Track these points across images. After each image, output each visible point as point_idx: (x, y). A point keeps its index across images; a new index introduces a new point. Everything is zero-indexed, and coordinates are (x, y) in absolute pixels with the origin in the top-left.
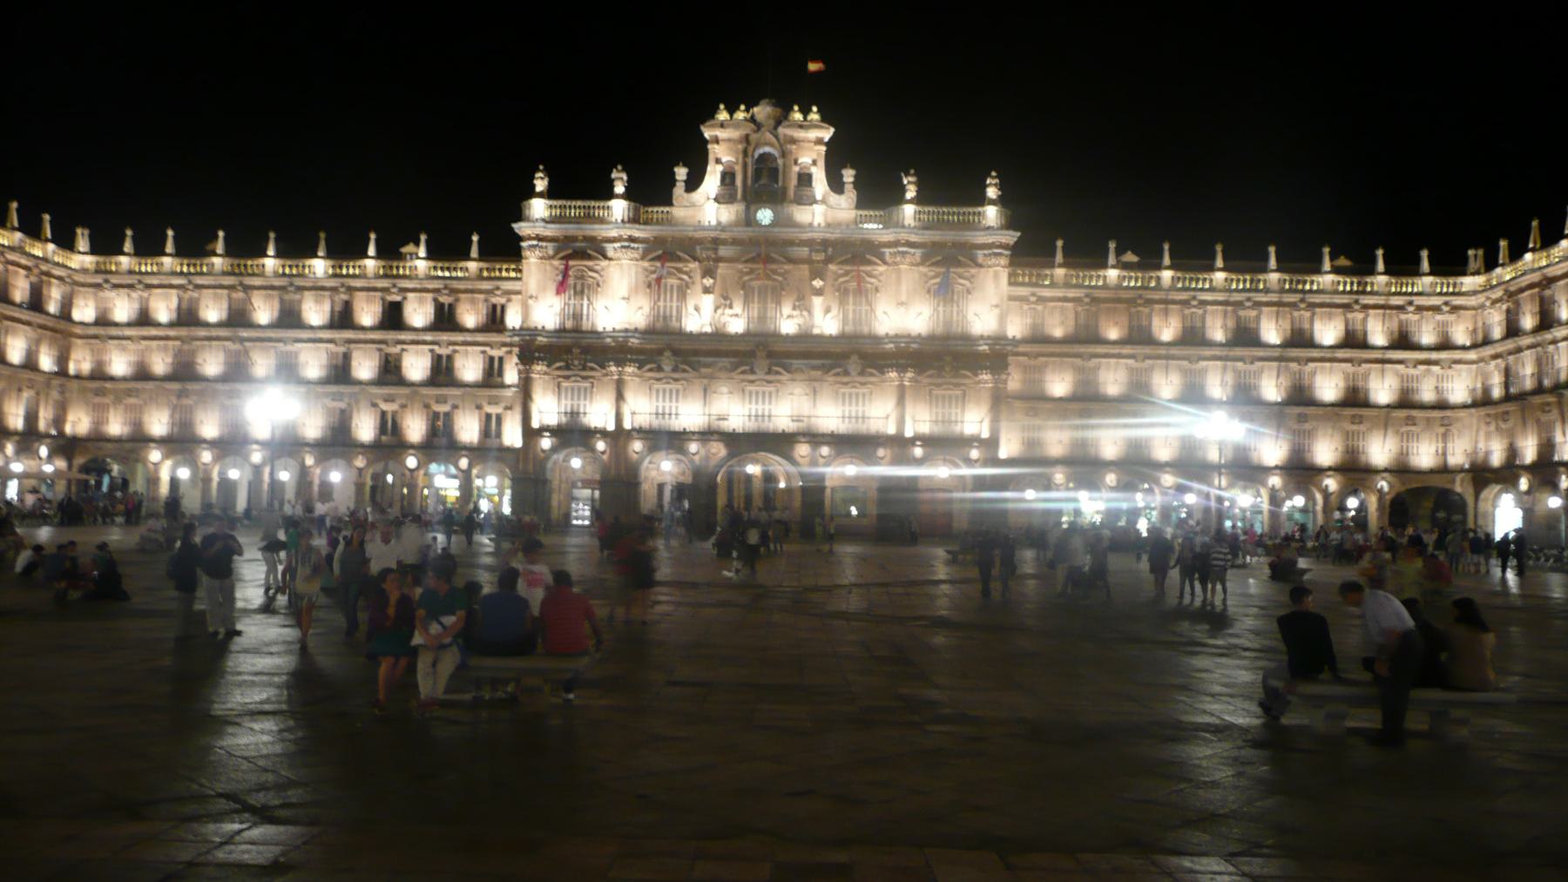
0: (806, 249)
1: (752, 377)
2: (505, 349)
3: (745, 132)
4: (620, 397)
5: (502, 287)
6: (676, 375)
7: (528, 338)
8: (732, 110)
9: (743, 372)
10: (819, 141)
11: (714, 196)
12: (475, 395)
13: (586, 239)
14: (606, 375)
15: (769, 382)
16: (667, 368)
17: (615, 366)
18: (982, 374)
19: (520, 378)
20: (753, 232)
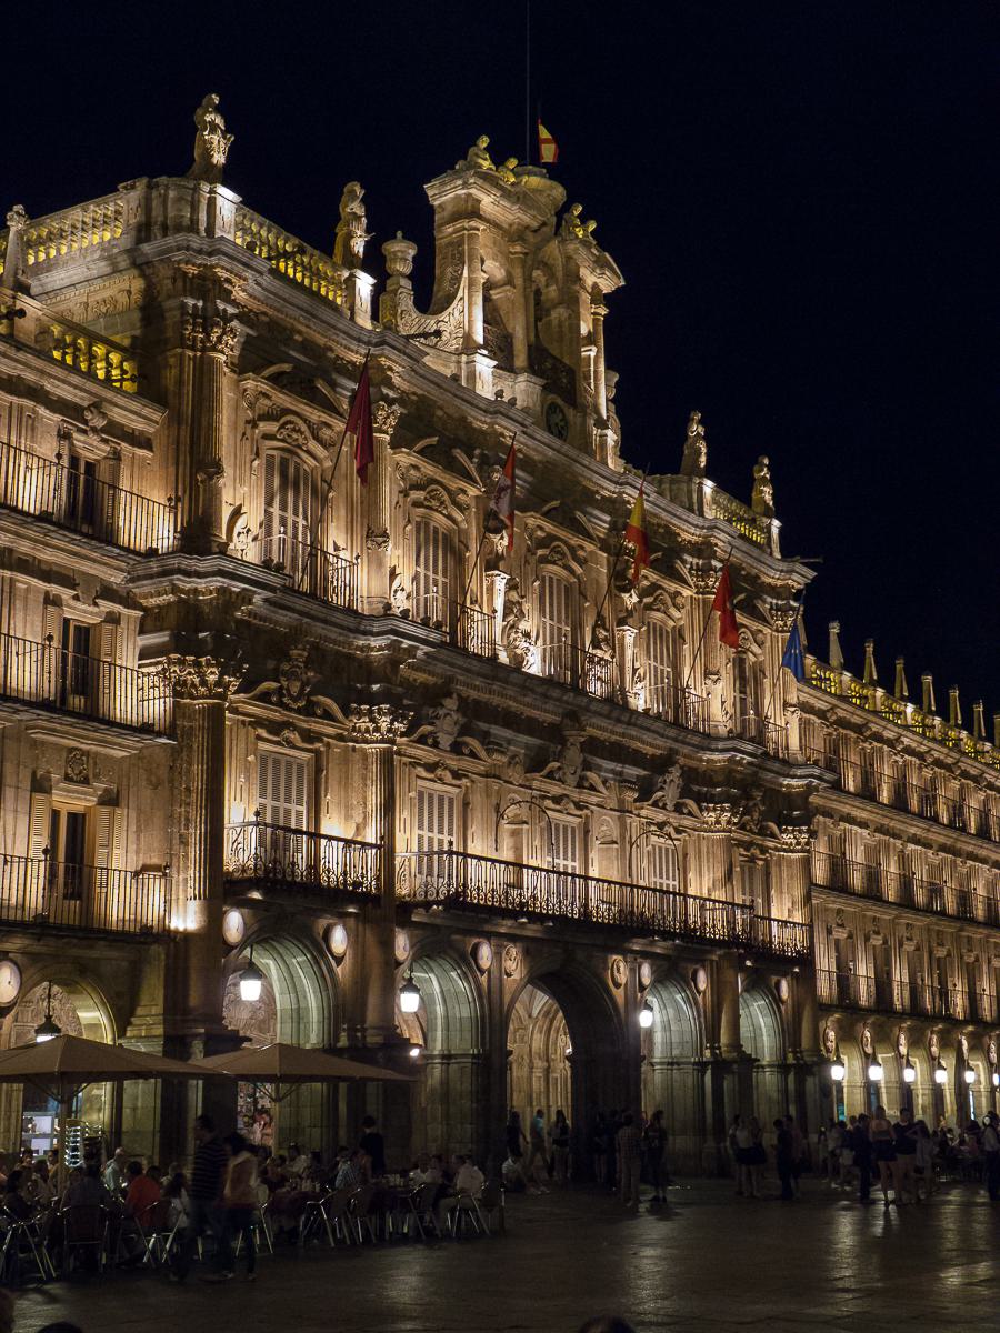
0: (608, 518)
1: (556, 790)
2: (106, 606)
3: (527, 219)
4: (388, 808)
5: (107, 408)
6: (453, 762)
7: (237, 587)
8: (499, 161)
9: (550, 775)
10: (597, 296)
11: (479, 338)
12: (34, 744)
13: (308, 347)
14: (340, 738)
15: (579, 806)
16: (445, 741)
17: (390, 712)
18: (786, 831)
19: (176, 704)
20: (558, 452)
